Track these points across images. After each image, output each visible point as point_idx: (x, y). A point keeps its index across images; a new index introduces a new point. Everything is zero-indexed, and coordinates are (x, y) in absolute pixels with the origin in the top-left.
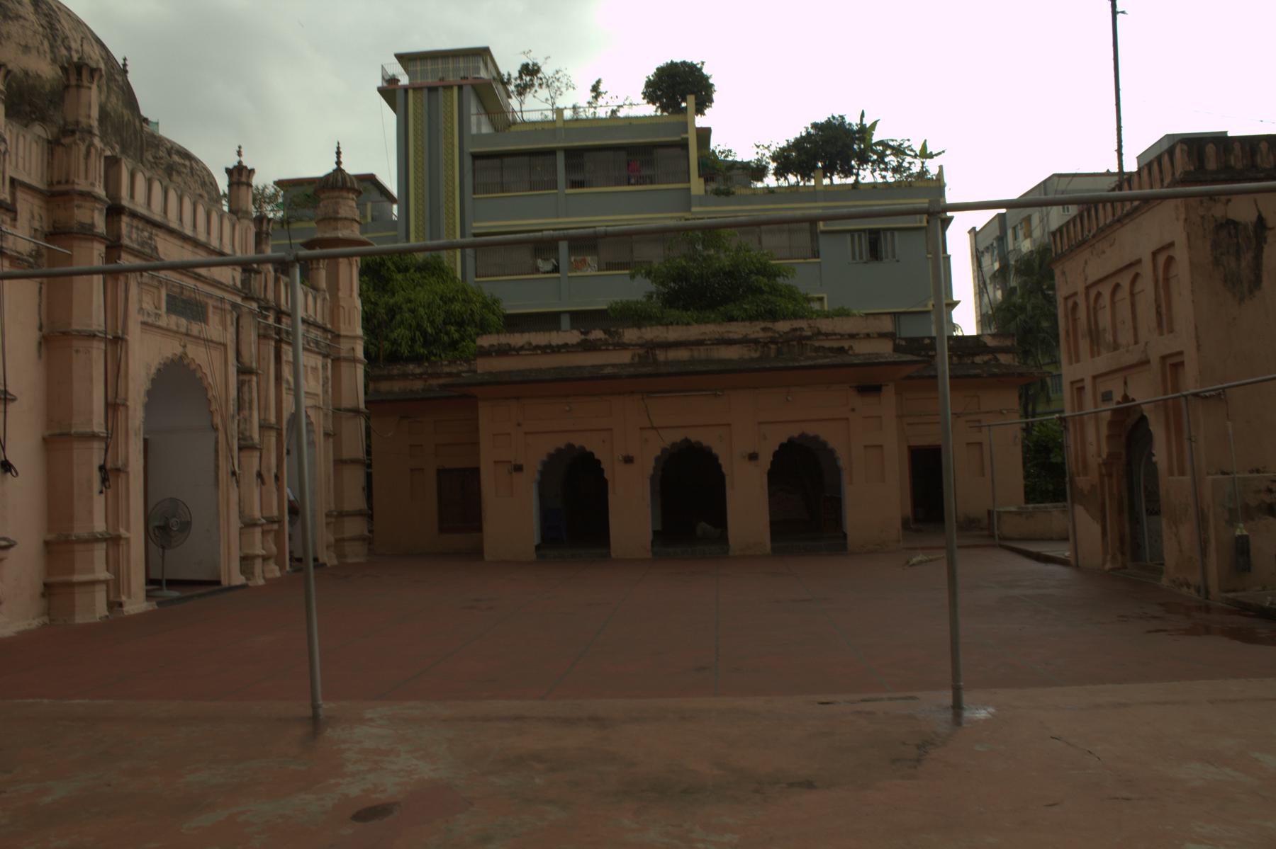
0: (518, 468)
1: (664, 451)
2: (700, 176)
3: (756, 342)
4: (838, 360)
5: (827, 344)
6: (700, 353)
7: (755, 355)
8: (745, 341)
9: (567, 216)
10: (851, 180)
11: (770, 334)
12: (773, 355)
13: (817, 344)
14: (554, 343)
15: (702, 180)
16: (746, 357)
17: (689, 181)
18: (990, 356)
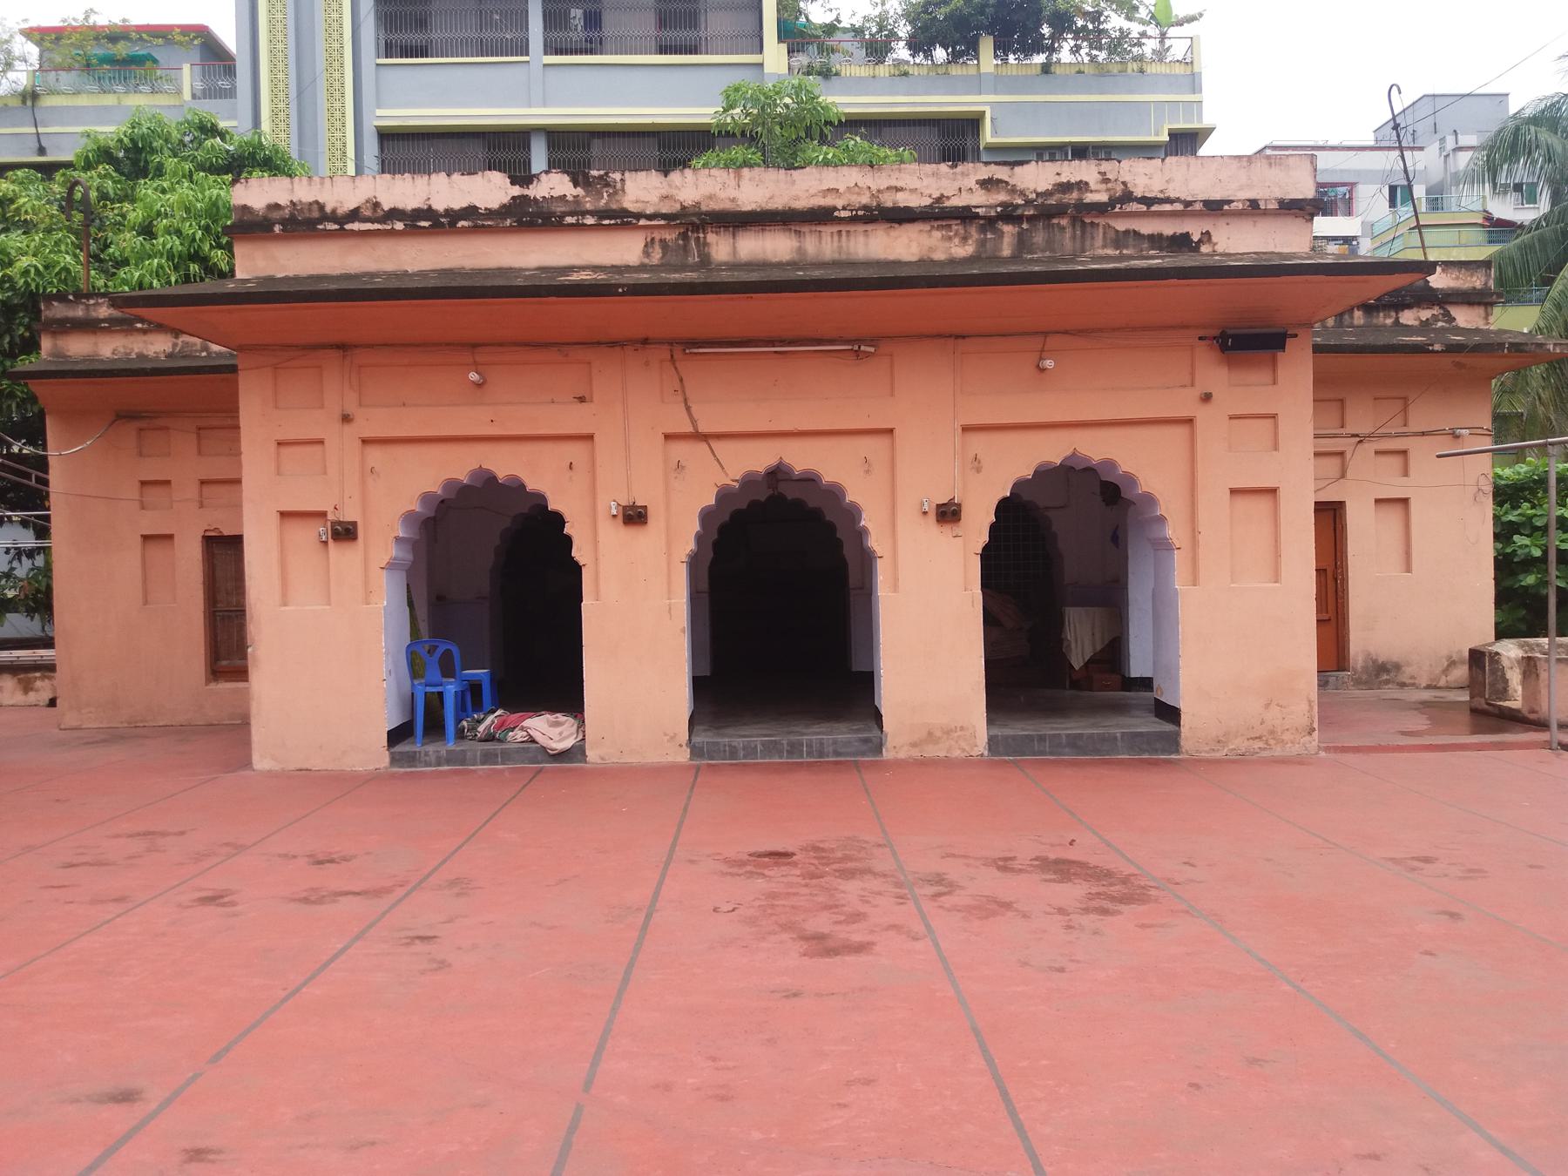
0: (345, 533)
1: (724, 495)
2: (780, 40)
3: (965, 215)
4: (1185, 260)
5: (1147, 227)
6: (822, 246)
7: (963, 251)
8: (937, 215)
9: (545, 105)
10: (1040, 59)
11: (1002, 197)
12: (1006, 252)
13: (1121, 225)
14: (439, 206)
15: (784, 47)
16: (939, 256)
17: (761, 51)
18: (1436, 311)
